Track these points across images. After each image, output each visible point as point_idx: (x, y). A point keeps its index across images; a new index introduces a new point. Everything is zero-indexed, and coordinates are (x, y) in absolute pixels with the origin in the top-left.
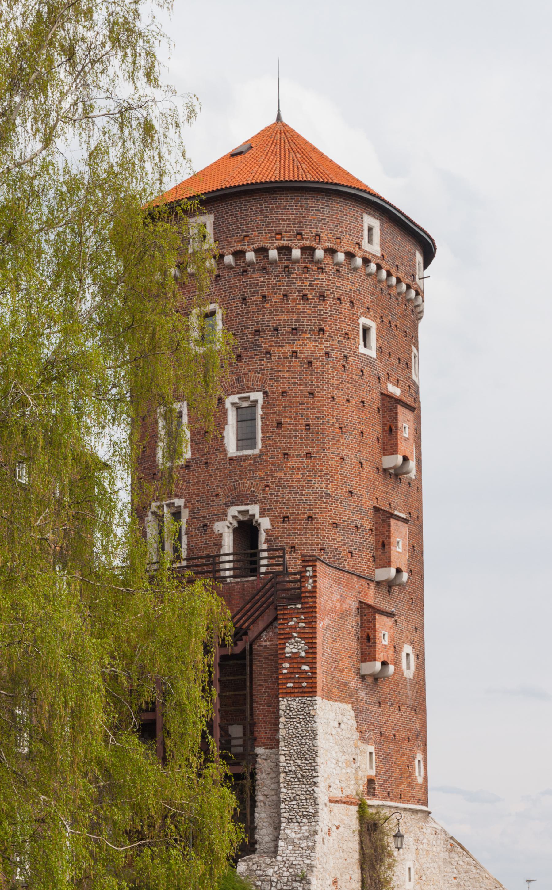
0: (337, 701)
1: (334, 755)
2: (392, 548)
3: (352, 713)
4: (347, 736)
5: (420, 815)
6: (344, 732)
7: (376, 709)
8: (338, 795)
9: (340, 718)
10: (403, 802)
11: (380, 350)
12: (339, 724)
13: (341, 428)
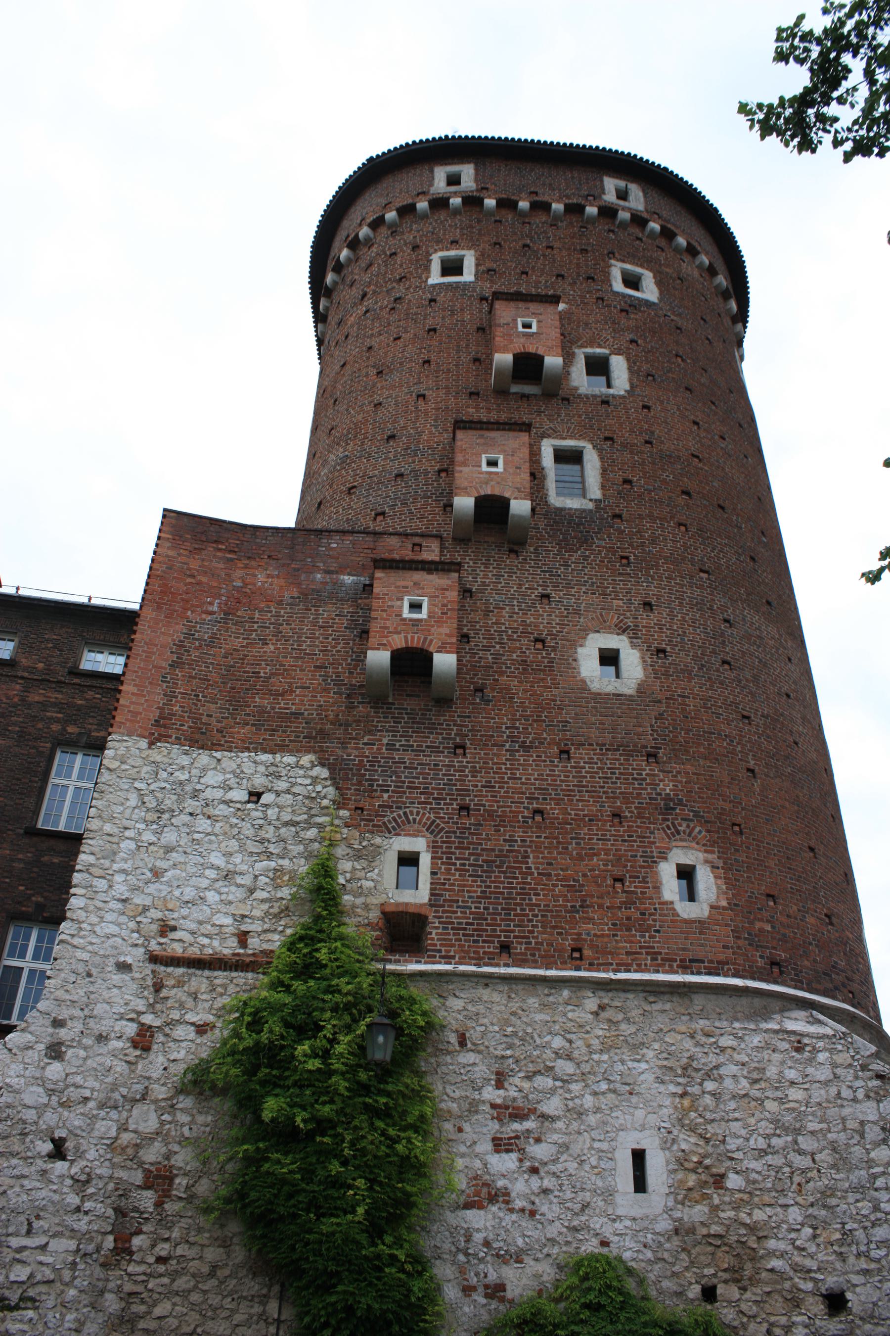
0: (248, 749)
1: (217, 859)
2: (457, 468)
3: (325, 773)
4: (286, 817)
5: (699, 1000)
6: (272, 813)
7: (443, 759)
8: (228, 948)
9: (259, 782)
10: (591, 967)
12: (255, 796)
13: (381, 372)
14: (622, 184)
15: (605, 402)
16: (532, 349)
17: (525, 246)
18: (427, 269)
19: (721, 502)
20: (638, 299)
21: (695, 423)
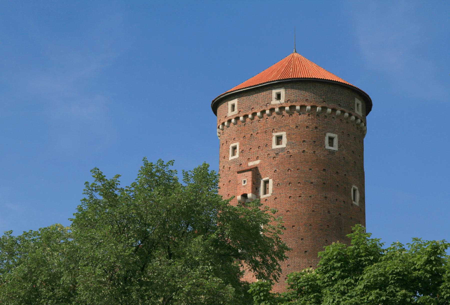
11: (242, 152)
14: (278, 91)
15: (266, 200)
16: (245, 193)
17: (252, 135)
18: (229, 153)
19: (294, 225)
20: (279, 149)
21: (290, 197)
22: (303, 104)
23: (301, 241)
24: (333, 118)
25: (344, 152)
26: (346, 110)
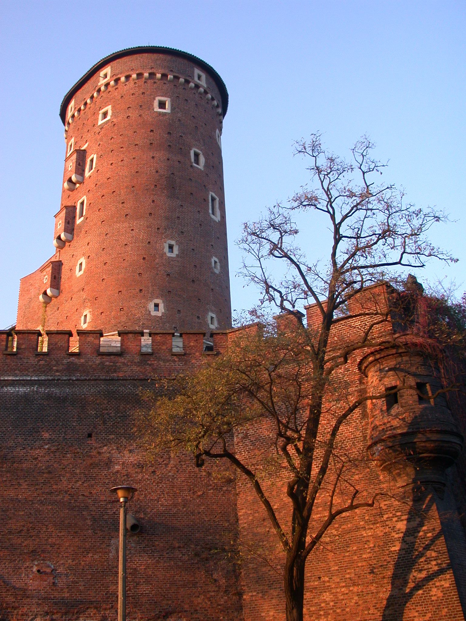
22: (128, 74)
23: (121, 205)
24: (165, 83)
25: (179, 115)
26: (180, 76)
